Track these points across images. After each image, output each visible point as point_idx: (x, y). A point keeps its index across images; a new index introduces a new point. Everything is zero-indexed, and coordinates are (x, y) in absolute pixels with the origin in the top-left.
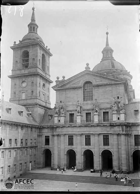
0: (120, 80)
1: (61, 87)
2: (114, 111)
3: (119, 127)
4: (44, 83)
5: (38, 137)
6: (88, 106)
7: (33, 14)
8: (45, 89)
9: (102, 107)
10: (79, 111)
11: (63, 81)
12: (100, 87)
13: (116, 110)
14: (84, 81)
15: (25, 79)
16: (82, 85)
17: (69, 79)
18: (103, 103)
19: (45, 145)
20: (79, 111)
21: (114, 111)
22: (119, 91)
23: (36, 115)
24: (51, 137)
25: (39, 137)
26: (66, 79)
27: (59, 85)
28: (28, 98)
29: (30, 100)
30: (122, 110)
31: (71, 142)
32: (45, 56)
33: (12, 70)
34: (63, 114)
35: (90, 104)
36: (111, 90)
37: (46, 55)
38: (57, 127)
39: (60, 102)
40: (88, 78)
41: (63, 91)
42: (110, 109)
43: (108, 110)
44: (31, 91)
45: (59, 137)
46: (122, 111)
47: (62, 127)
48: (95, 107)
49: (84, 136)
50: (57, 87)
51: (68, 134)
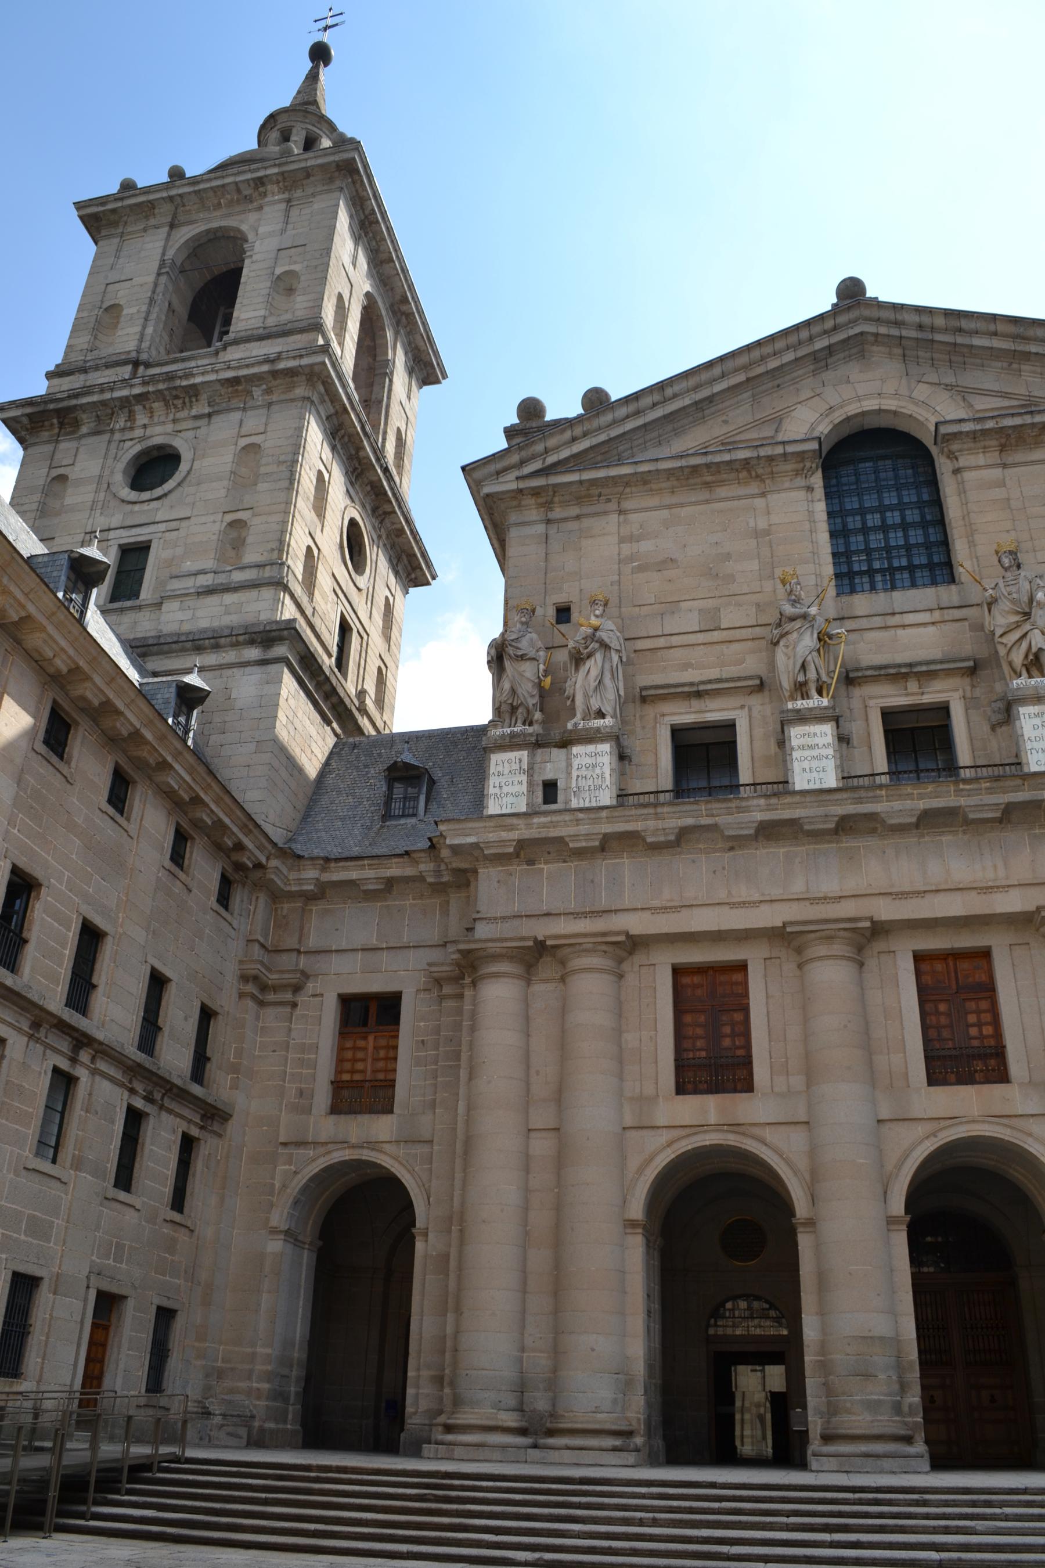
5: (241, 995)
7: (313, 77)
8: (362, 581)
10: (812, 675)
12: (1019, 456)
15: (170, 427)
19: (335, 1109)
20: (804, 667)
23: (252, 747)
25: (262, 1004)
28: (176, 585)
29: (191, 602)
31: (713, 1053)
32: (389, 335)
33: (51, 368)
34: (601, 715)
37: (397, 333)
39: (551, 612)
40: (873, 390)
41: (586, 510)
44: (217, 527)
45: (543, 991)
48: (1017, 618)
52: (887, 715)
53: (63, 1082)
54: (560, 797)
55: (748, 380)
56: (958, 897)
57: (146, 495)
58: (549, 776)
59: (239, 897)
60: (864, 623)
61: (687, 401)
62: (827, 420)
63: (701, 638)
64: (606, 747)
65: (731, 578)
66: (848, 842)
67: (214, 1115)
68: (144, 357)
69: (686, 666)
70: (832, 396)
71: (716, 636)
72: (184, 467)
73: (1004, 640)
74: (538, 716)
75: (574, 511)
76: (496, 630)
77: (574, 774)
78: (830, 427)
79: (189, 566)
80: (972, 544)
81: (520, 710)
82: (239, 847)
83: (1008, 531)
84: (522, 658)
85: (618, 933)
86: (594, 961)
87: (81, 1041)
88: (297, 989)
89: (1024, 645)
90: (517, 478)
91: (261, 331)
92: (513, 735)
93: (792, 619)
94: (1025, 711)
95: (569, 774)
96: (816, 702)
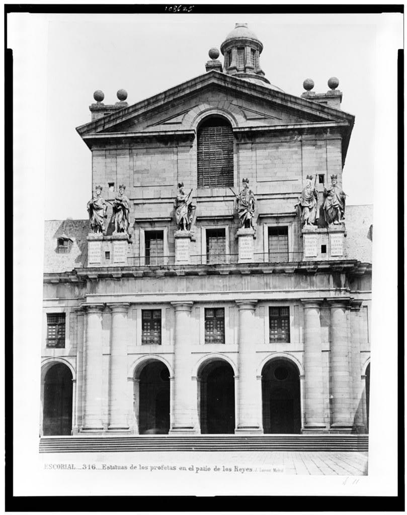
0: (332, 115)
1: (115, 129)
2: (308, 224)
3: (327, 276)
9: (267, 207)
10: (185, 222)
11: (119, 111)
12: (257, 140)
13: (316, 220)
14: (202, 113)
16: (195, 127)
17: (146, 103)
20: (182, 219)
21: (308, 224)
22: (324, 156)
24: (73, 316)
26: (130, 101)
27: (106, 120)
30: (334, 221)
34: (122, 230)
35: (222, 199)
38: (101, 277)
42: (294, 217)
43: (286, 220)
45: (107, 315)
46: (336, 222)
47: (118, 279)
48: (242, 208)
49: (203, 311)
50: (96, 128)
51: (141, 304)
52: (207, 230)
54: (111, 257)
55: (174, 99)
62: (200, 117)
65: (165, 179)
70: (203, 107)
73: (240, 214)
75: (115, 147)
76: (89, 199)
77: (115, 249)
78: (201, 119)
80: (239, 173)
81: (98, 227)
83: (250, 169)
85: (126, 303)
86: (120, 310)
89: (245, 217)
93: (181, 202)
94: (241, 239)
95: (113, 250)
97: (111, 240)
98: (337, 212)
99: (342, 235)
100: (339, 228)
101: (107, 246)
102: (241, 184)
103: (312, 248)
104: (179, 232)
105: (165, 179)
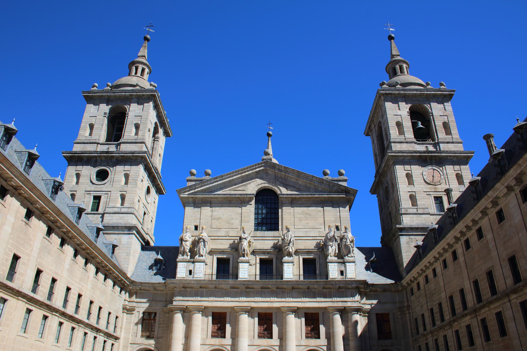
4: (149, 185)
5: (123, 312)
6: (266, 241)
14: (258, 185)
18: (302, 238)
20: (244, 250)
25: (127, 314)
28: (108, 210)
34: (202, 256)
36: (320, 211)
46: (349, 255)
53: (95, 338)
56: (267, 303)
57: (100, 183)
58: (190, 269)
59: (123, 292)
60: (258, 238)
61: (227, 180)
63: (225, 238)
64: (202, 264)
65: (233, 224)
66: (248, 290)
67: (117, 338)
68: (101, 142)
69: (221, 244)
71: (228, 238)
72: (109, 176)
74: (189, 254)
79: (111, 205)
80: (282, 222)
82: (125, 282)
84: (186, 241)
87: (98, 330)
88: (134, 310)
90: (189, 194)
91: (130, 141)
92: (183, 259)
94: (285, 264)
96: (246, 258)
97: (193, 262)
98: (350, 249)
99: (353, 264)
100: (351, 259)
101: (191, 266)
102: (284, 229)
103: (334, 272)
104: (242, 258)
105: (233, 224)
